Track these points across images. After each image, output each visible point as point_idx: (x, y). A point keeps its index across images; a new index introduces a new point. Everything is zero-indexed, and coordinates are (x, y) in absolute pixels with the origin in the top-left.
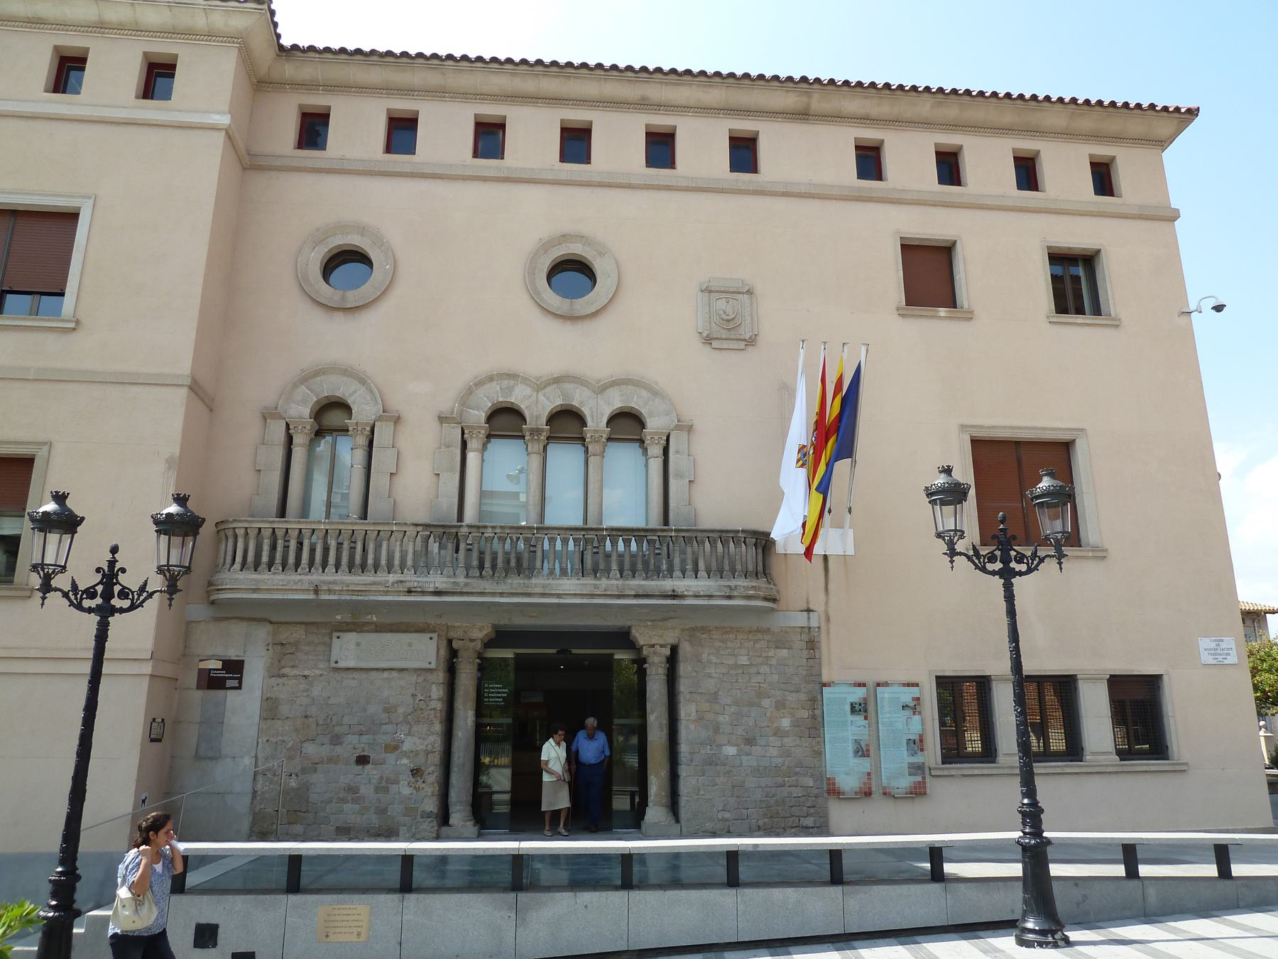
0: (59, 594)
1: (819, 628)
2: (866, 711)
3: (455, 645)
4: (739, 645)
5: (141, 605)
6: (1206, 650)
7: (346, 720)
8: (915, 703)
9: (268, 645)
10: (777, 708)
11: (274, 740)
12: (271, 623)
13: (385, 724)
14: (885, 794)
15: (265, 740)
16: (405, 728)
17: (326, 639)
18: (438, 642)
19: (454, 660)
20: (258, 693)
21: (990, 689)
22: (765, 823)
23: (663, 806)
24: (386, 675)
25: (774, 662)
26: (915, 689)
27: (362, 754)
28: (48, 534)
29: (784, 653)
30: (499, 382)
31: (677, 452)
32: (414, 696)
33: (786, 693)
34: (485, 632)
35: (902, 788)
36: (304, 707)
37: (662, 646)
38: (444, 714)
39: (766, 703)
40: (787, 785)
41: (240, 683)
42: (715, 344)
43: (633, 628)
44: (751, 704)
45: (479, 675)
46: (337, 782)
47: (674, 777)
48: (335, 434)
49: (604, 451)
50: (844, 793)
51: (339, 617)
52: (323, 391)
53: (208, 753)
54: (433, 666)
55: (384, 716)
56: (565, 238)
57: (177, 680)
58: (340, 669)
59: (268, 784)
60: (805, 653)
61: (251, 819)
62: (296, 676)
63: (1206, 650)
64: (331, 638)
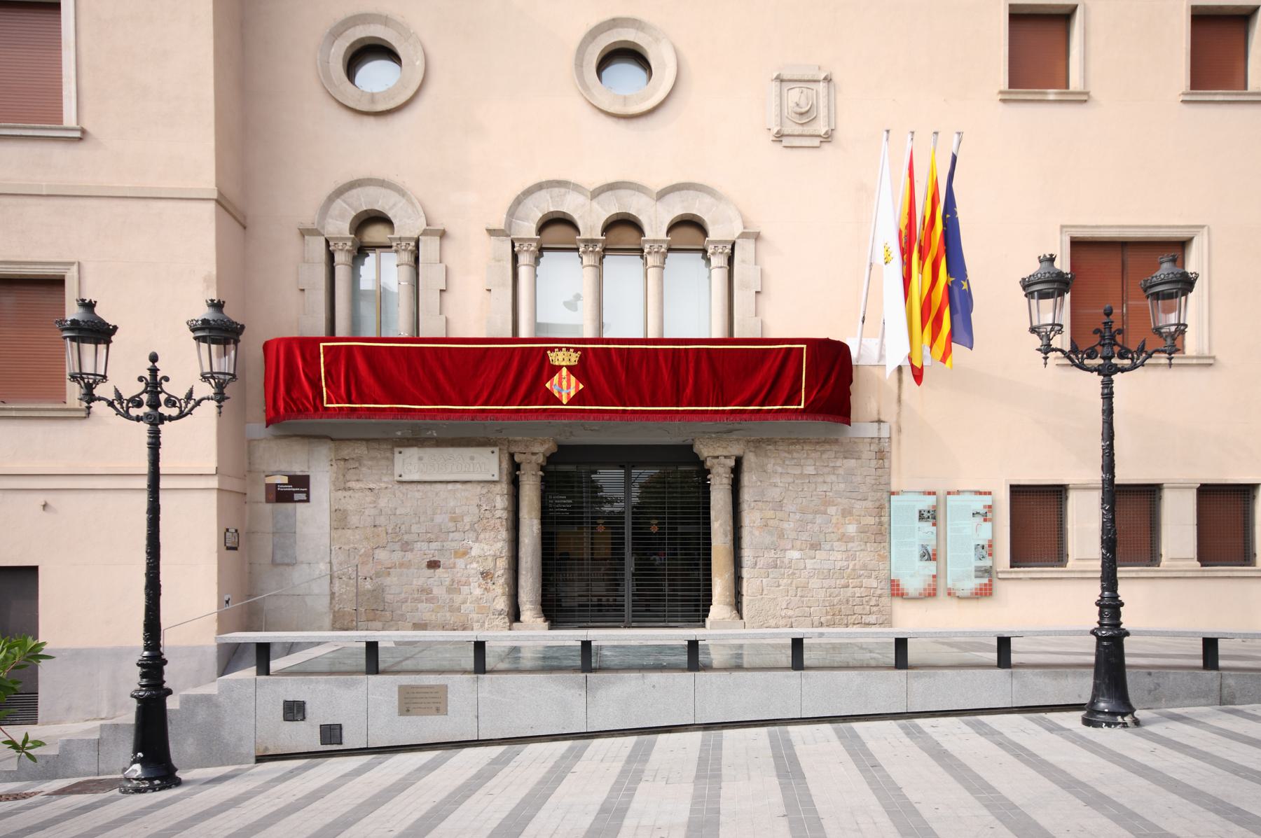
0: (104, 403)
1: (890, 438)
2: (934, 518)
3: (517, 459)
4: (805, 455)
5: (190, 412)
7: (415, 528)
8: (987, 510)
9: (331, 460)
10: (844, 515)
11: (347, 547)
12: (332, 440)
13: (453, 532)
14: (949, 594)
15: (338, 547)
16: (472, 535)
17: (388, 454)
18: (500, 456)
19: (517, 473)
20: (326, 506)
21: (1067, 498)
22: (827, 621)
23: (727, 605)
24: (450, 486)
25: (841, 471)
27: (432, 559)
28: (81, 344)
30: (549, 190)
31: (743, 261)
32: (479, 506)
33: (853, 501)
34: (546, 446)
35: (967, 590)
36: (372, 518)
37: (726, 457)
38: (510, 523)
39: (832, 510)
40: (851, 586)
41: (308, 496)
42: (786, 141)
43: (697, 440)
44: (816, 512)
45: (543, 487)
46: (411, 585)
47: (738, 579)
48: (378, 250)
49: (664, 263)
50: (907, 594)
51: (399, 433)
52: (361, 205)
53: (284, 560)
54: (496, 478)
55: (451, 524)
56: (614, 23)
57: (245, 494)
58: (405, 482)
59: (344, 586)
60: (874, 463)
61: (331, 616)
62: (361, 490)
64: (394, 454)
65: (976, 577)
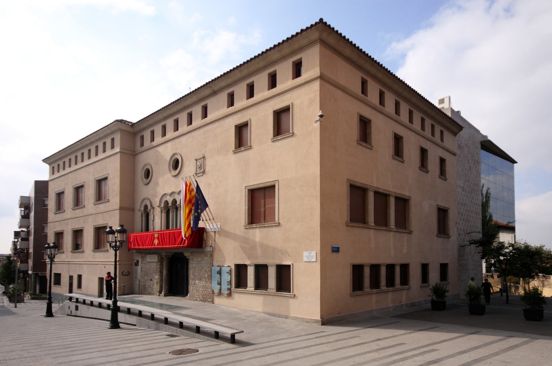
6: (305, 256)
26: (229, 268)
29: (206, 258)
63: (305, 256)
65: (227, 290)
